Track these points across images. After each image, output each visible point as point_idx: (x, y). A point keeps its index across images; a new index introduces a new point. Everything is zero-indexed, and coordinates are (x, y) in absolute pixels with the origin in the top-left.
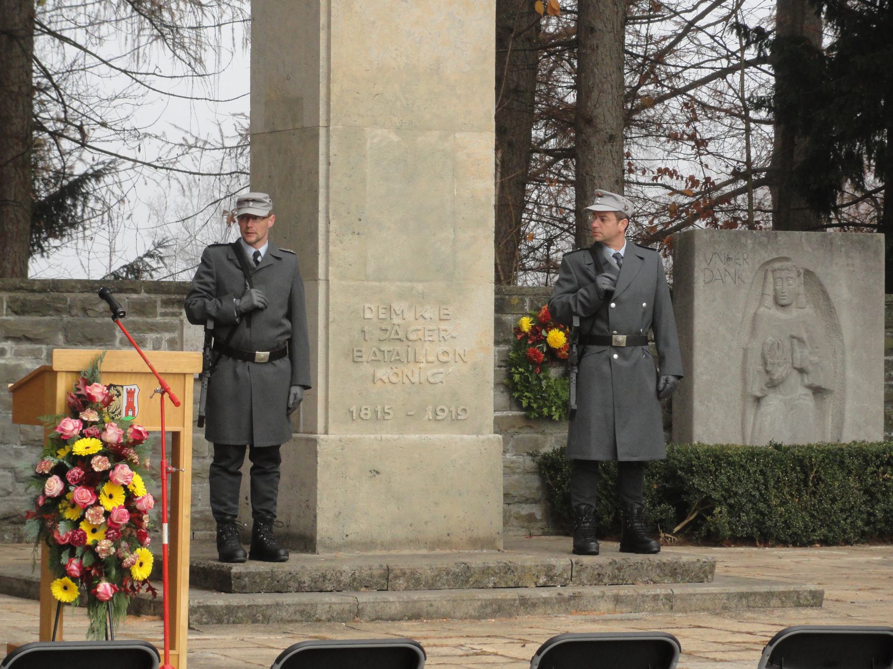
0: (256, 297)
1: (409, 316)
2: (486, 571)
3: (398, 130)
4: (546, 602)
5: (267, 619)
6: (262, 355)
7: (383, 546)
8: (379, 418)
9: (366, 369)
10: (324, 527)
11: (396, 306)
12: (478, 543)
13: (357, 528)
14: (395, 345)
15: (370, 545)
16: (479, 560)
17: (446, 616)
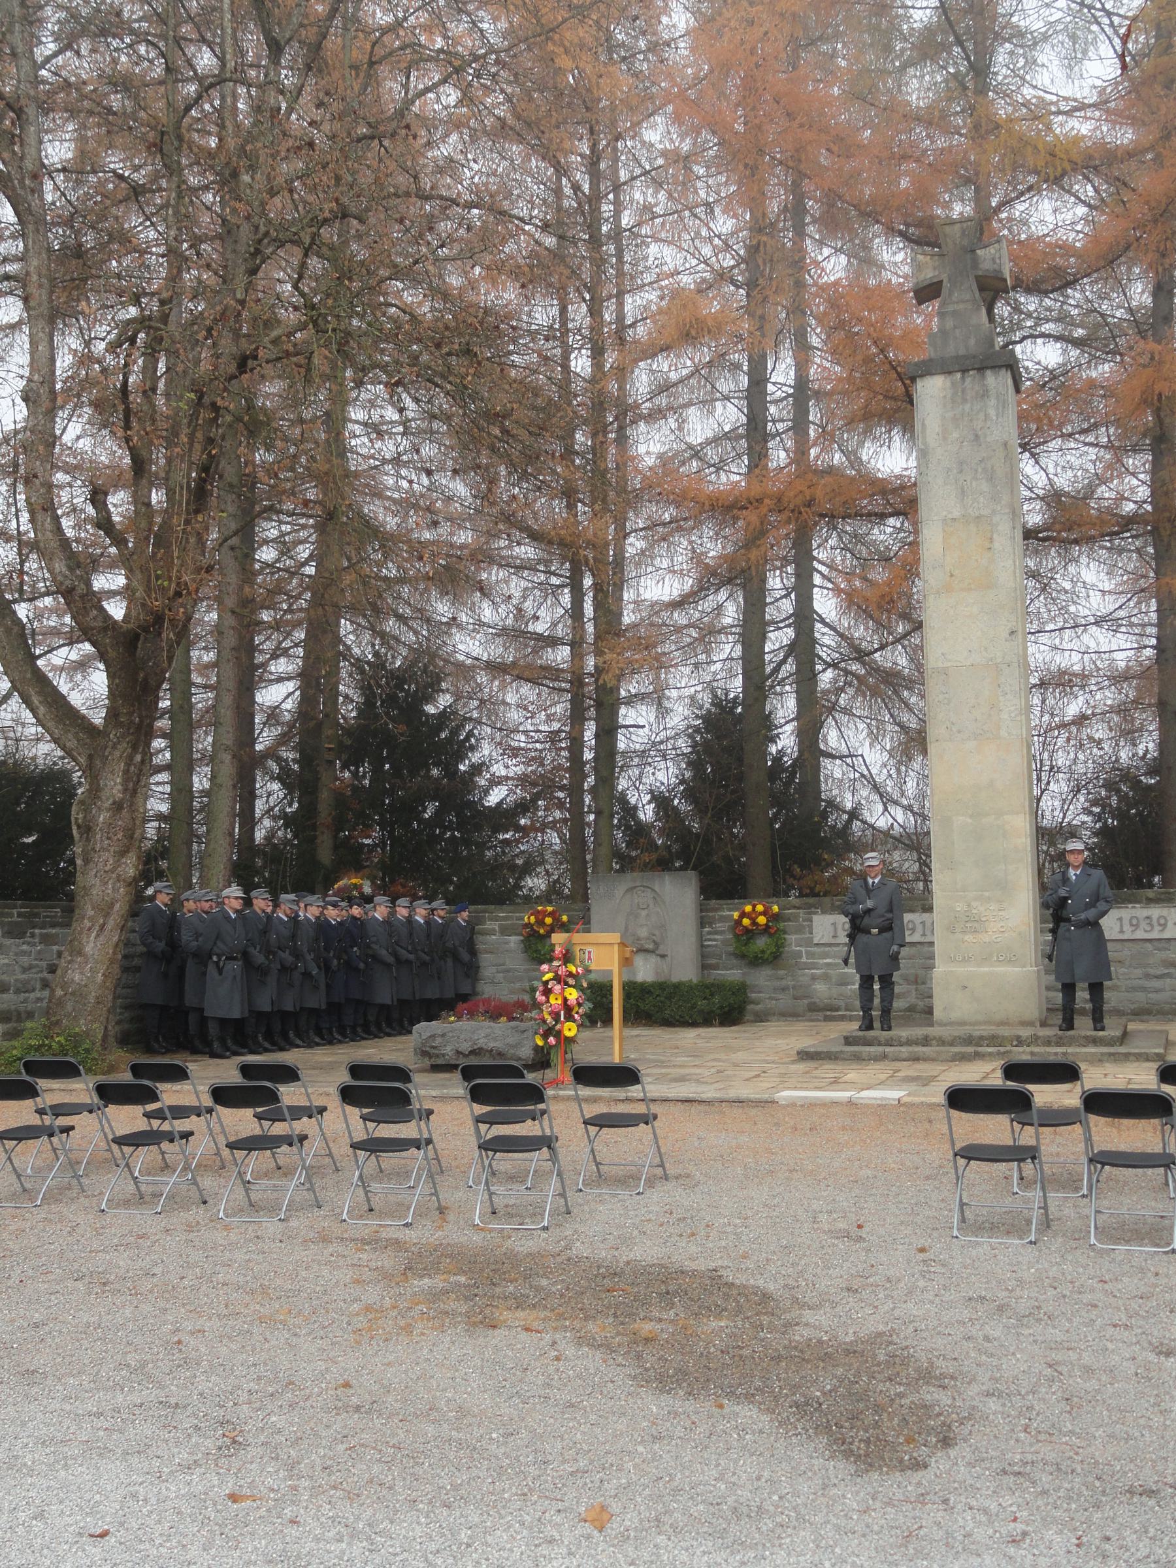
0: (870, 904)
1: (982, 909)
2: (981, 1038)
3: (971, 817)
4: (990, 1054)
5: (836, 1058)
6: (875, 931)
7: (971, 1024)
8: (966, 960)
9: (959, 936)
10: (938, 1013)
11: (974, 904)
12: (1024, 1024)
13: (955, 1015)
14: (973, 924)
15: (963, 1023)
16: (1025, 1033)
17: (933, 1060)
